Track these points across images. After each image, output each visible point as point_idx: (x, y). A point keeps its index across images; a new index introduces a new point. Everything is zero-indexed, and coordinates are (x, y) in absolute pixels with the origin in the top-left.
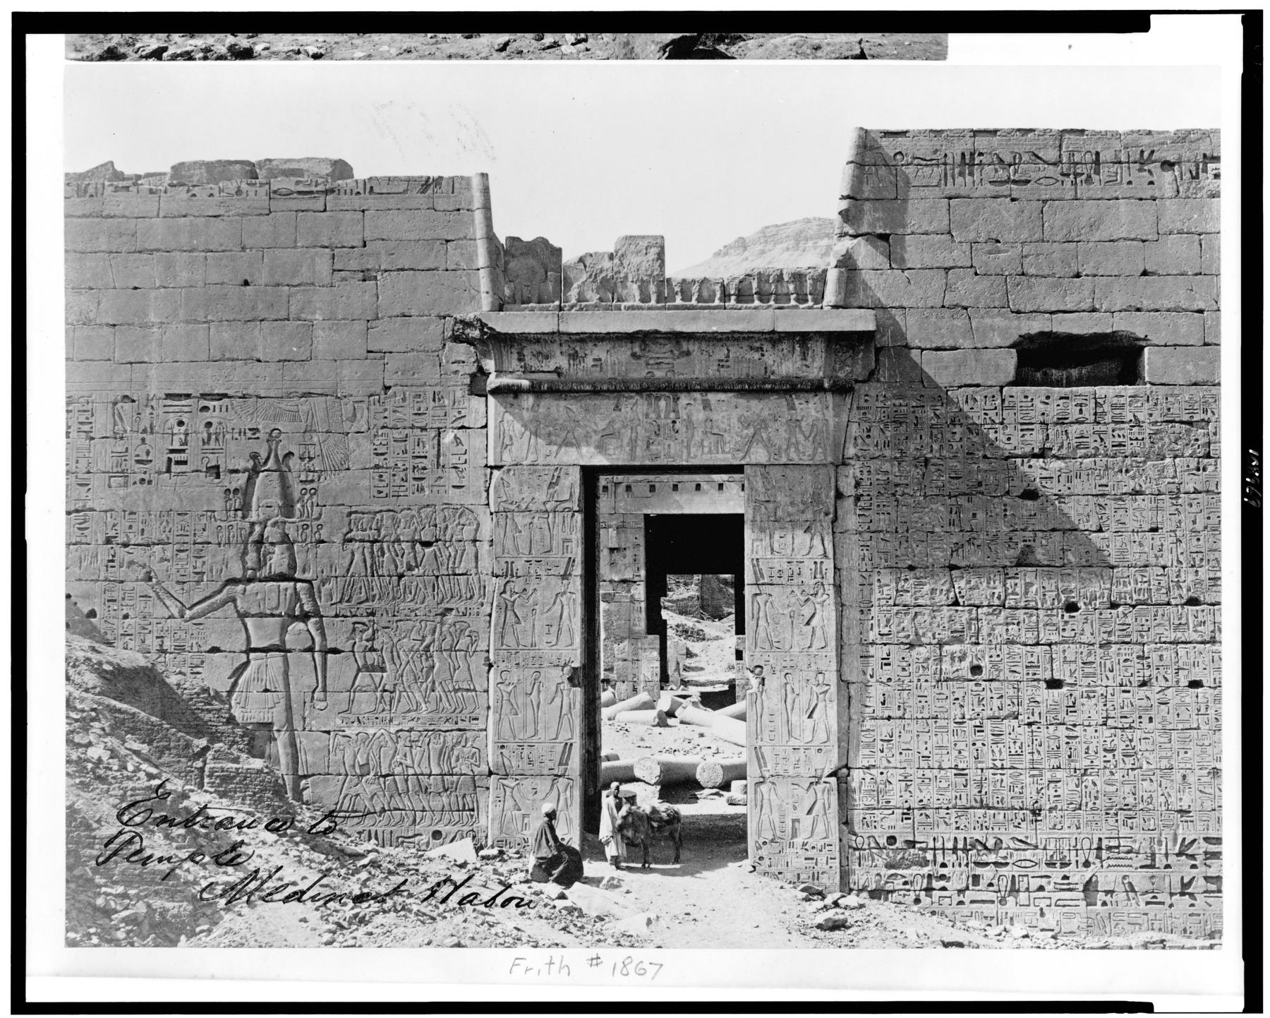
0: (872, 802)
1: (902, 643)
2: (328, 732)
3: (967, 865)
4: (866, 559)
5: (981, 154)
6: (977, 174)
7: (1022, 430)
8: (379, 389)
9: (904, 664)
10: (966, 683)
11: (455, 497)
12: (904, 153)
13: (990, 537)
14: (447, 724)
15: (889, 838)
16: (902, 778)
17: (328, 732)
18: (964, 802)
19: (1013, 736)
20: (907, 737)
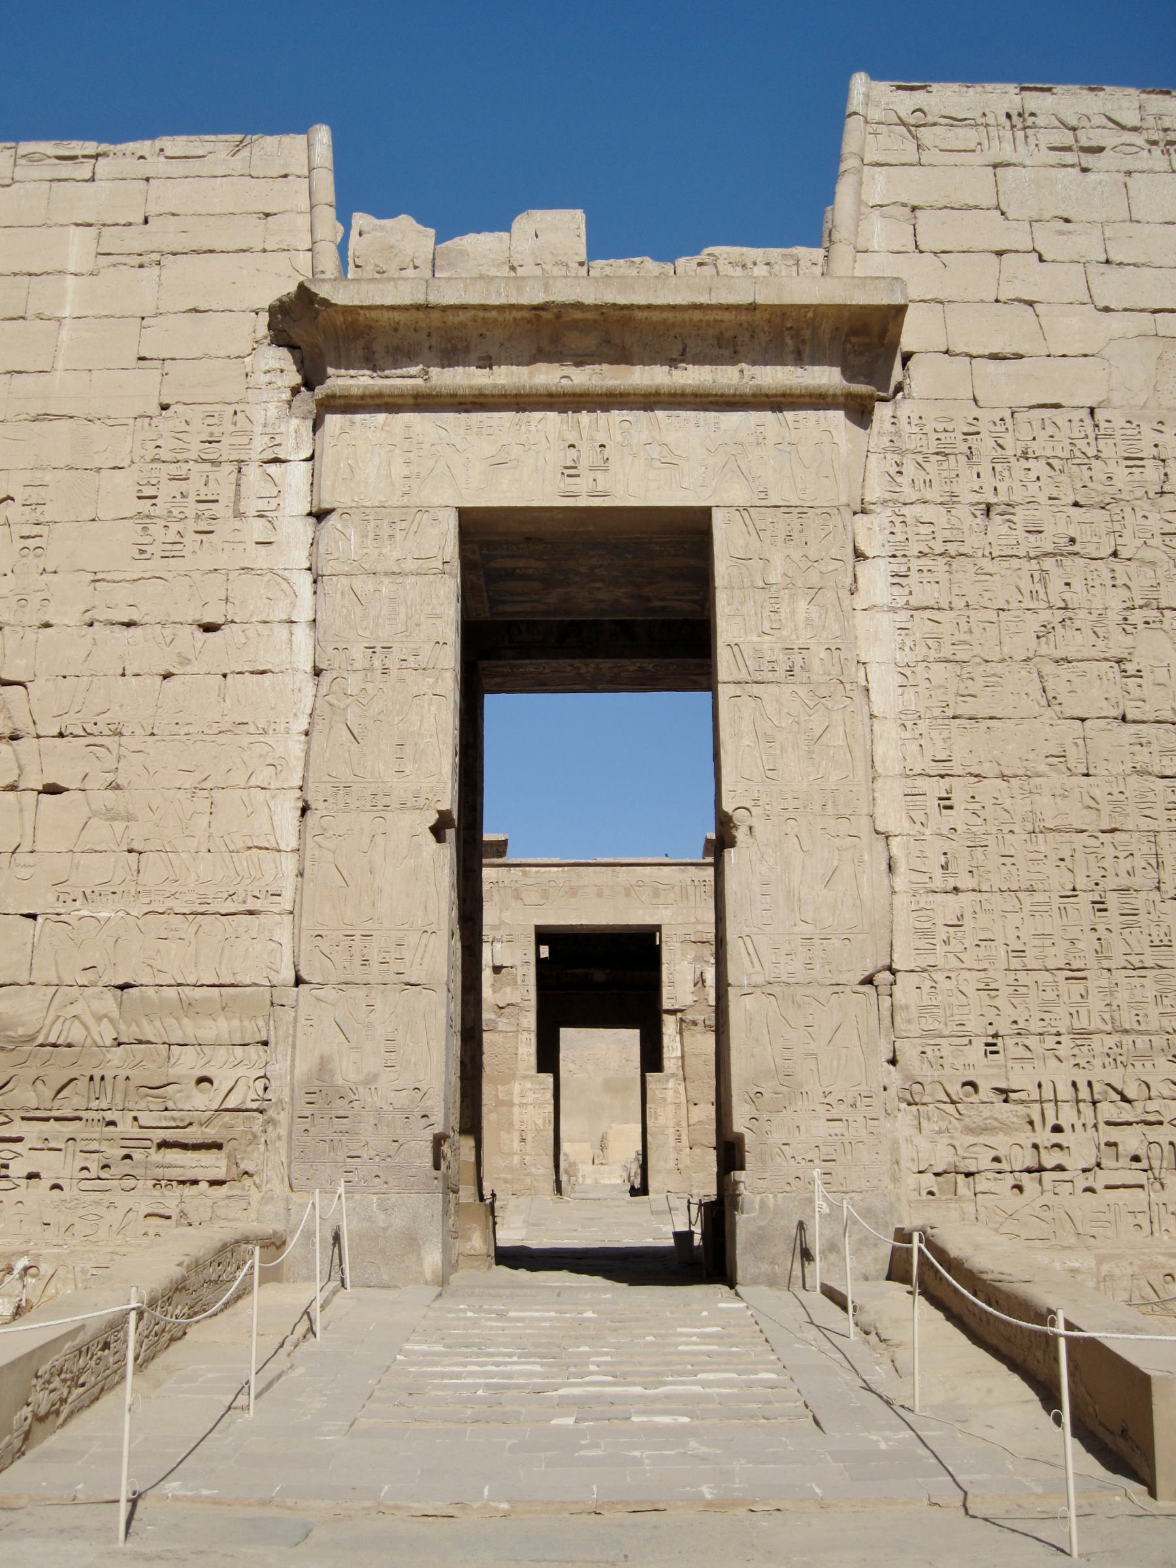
0: (936, 1025)
1: (971, 775)
2: (34, 917)
3: (1095, 1126)
4: (907, 649)
5: (1032, 114)
6: (1032, 140)
7: (1127, 467)
8: (154, 410)
9: (976, 806)
10: (1075, 835)
11: (261, 558)
12: (926, 109)
13: (1094, 617)
14: (229, 903)
15: (965, 1084)
16: (982, 986)
17: (34, 917)
18: (1084, 1023)
19: (1153, 917)
20: (984, 919)
